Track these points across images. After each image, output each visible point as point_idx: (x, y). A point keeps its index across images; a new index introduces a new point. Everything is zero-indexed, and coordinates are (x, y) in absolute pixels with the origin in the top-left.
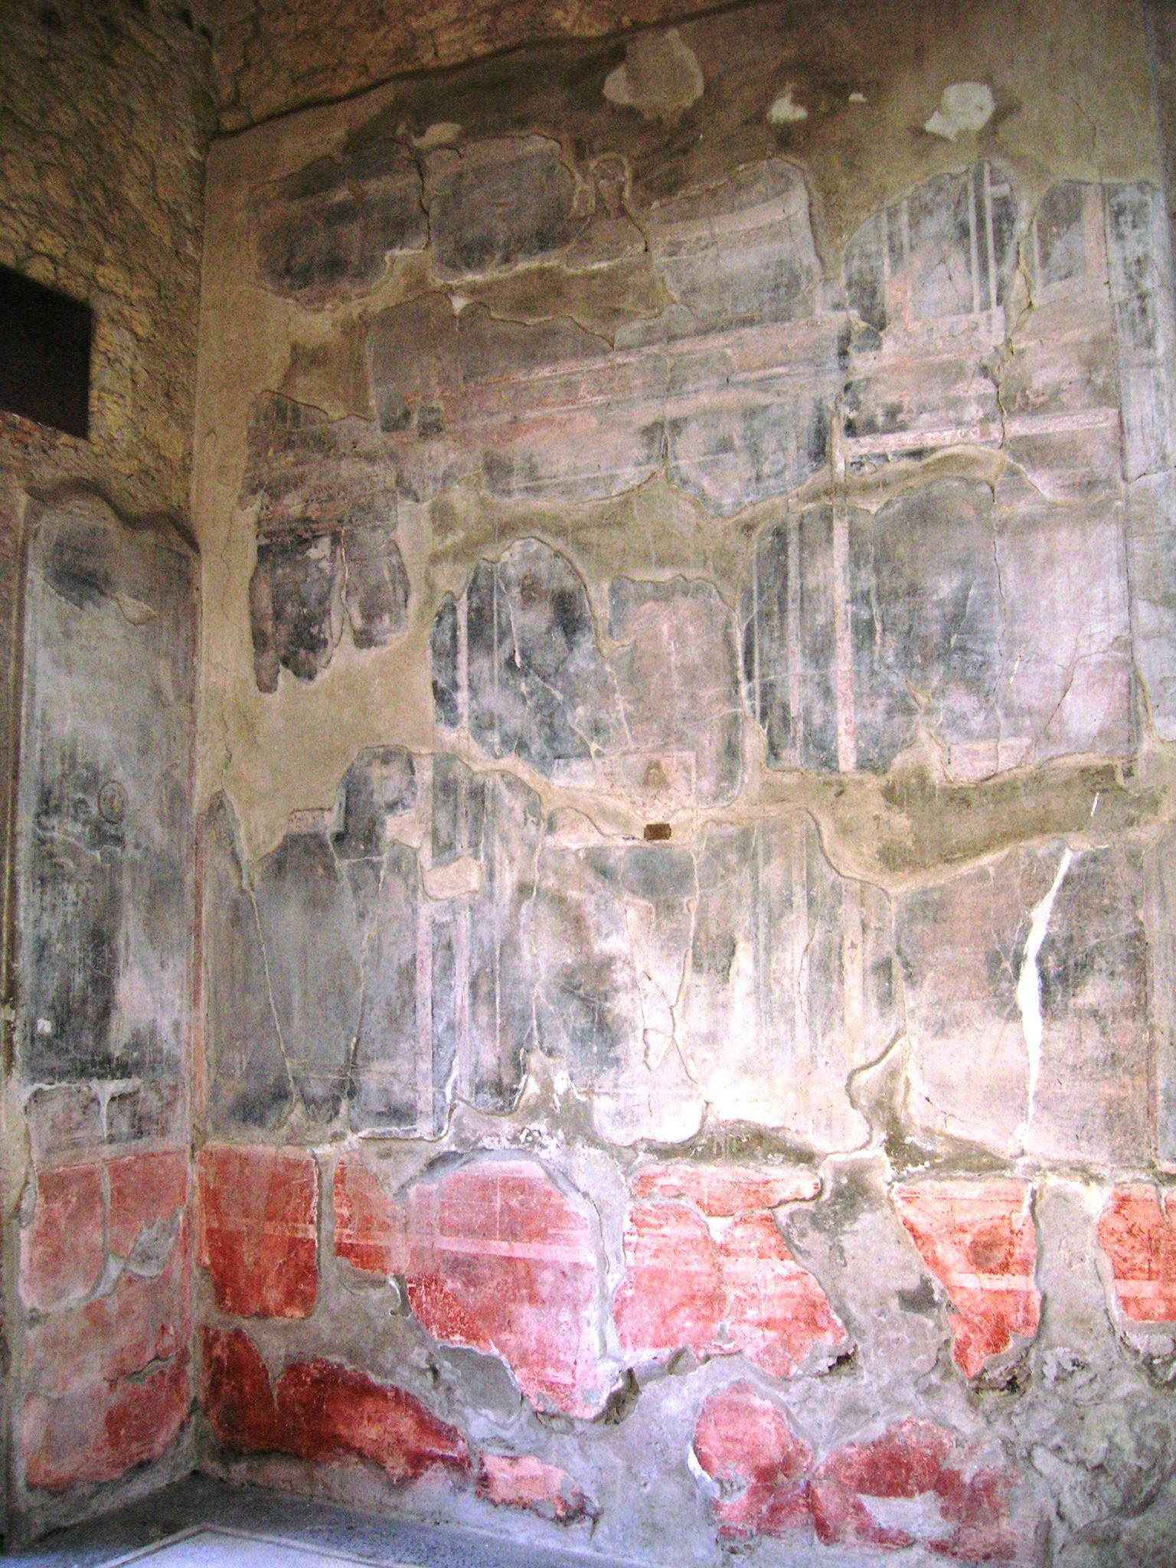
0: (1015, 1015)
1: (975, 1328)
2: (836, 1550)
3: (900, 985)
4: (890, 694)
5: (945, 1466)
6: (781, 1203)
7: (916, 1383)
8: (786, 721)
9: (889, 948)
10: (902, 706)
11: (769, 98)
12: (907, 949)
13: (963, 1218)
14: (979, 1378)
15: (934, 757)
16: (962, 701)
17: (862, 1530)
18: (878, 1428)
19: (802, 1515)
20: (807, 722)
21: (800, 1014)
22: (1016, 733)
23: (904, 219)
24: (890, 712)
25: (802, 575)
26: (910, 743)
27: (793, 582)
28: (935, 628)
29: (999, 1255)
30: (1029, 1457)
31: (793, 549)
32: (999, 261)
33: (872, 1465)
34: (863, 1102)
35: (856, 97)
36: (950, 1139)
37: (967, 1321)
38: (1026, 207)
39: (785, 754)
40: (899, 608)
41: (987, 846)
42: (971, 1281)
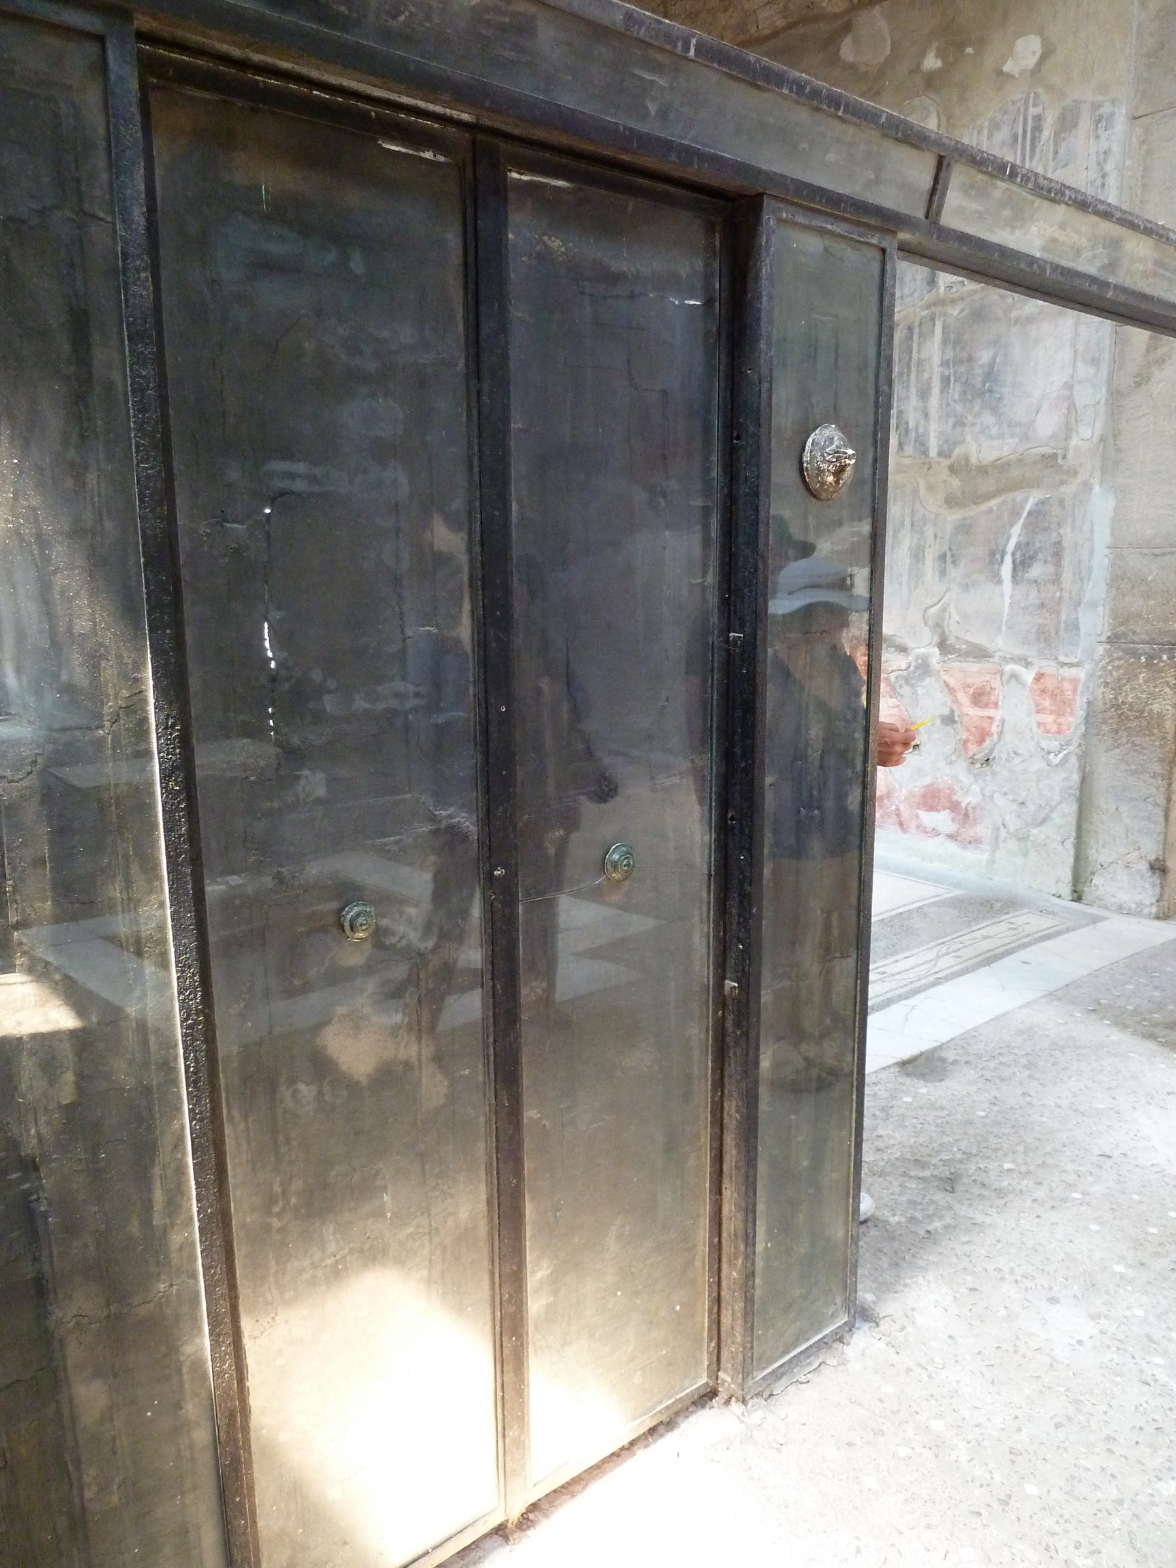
0: (999, 582)
1: (972, 734)
2: (907, 836)
3: (949, 566)
4: (955, 416)
5: (955, 798)
6: (892, 671)
7: (946, 759)
8: (907, 430)
9: (946, 548)
10: (960, 423)
11: (923, 54)
12: (954, 548)
13: (969, 681)
14: (972, 758)
15: (974, 448)
16: (988, 419)
17: (918, 827)
18: (927, 780)
19: (894, 819)
20: (916, 431)
21: (905, 579)
22: (1012, 436)
23: (986, 132)
24: (954, 426)
25: (919, 352)
26: (962, 442)
27: (915, 355)
28: (979, 379)
29: (985, 699)
30: (992, 797)
31: (916, 337)
32: (1032, 157)
33: (924, 796)
34: (930, 623)
35: (969, 50)
36: (967, 642)
37: (968, 730)
38: (1050, 120)
39: (905, 448)
40: (962, 369)
41: (993, 495)
42: (973, 712)
